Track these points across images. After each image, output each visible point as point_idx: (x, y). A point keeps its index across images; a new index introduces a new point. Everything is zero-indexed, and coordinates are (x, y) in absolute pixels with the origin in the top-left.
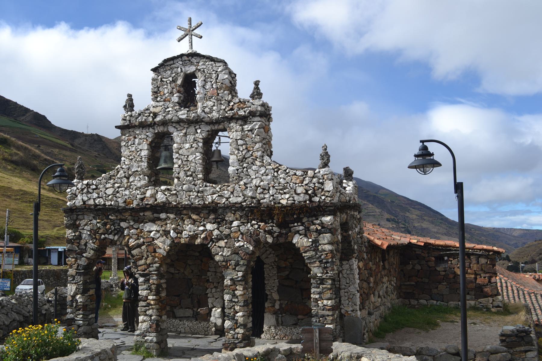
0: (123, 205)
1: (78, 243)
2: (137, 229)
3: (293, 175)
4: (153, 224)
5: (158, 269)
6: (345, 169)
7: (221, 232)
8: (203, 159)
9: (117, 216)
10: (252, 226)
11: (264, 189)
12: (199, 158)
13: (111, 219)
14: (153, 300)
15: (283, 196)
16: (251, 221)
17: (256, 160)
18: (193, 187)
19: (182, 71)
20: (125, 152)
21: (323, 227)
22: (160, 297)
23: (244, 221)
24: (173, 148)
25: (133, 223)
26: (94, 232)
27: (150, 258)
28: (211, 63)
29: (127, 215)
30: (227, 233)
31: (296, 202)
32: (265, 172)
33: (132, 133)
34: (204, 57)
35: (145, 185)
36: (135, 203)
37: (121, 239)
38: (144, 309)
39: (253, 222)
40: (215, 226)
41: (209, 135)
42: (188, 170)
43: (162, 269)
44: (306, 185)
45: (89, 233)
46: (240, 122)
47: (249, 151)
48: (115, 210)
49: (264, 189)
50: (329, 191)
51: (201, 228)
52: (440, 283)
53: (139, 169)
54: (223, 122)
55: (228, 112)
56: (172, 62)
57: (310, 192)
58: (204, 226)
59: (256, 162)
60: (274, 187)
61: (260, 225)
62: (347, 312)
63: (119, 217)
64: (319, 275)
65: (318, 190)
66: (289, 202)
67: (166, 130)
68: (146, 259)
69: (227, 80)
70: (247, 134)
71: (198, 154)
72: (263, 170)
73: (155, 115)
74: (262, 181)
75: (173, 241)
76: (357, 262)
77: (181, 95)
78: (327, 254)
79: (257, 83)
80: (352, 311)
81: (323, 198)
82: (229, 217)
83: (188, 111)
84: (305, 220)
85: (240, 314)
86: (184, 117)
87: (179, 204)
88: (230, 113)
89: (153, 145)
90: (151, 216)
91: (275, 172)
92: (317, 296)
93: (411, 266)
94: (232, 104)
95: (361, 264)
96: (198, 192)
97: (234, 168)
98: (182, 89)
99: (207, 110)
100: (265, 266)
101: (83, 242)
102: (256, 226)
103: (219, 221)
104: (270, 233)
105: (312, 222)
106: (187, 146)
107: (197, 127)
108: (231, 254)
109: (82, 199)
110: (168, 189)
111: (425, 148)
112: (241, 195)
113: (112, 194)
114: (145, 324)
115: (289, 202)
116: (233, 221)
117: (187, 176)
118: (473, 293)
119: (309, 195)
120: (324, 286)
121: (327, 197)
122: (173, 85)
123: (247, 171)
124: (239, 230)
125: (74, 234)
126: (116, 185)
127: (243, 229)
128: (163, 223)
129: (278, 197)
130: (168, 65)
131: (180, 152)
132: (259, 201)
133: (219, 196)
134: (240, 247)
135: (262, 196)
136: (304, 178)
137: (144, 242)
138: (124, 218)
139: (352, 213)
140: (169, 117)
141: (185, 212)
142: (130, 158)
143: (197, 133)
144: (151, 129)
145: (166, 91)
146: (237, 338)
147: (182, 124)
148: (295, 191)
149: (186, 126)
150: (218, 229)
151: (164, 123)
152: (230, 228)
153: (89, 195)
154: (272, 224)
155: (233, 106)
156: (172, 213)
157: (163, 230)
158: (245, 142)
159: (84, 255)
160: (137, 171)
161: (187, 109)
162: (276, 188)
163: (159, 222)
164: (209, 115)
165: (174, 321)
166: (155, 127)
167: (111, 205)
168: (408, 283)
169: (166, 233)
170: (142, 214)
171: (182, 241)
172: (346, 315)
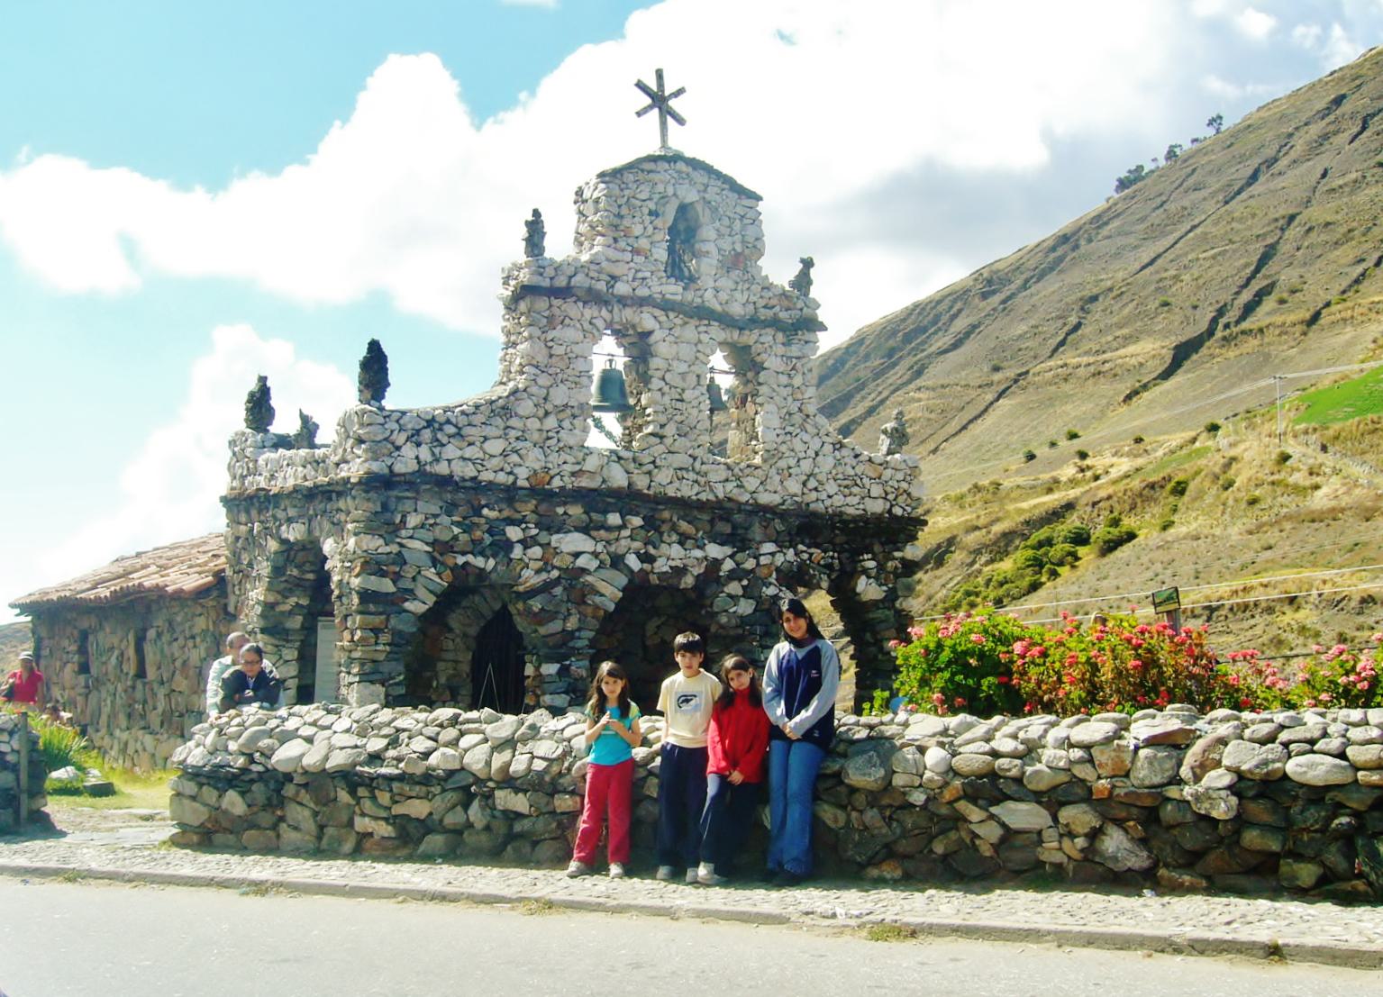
0: (526, 484)
1: (395, 573)
4: (584, 537)
7: (738, 564)
13: (487, 518)
15: (849, 500)
18: (691, 460)
19: (675, 194)
25: (536, 531)
26: (441, 549)
28: (731, 195)
34: (719, 175)
36: (557, 483)
39: (801, 547)
40: (728, 550)
46: (780, 336)
58: (702, 547)
61: (811, 555)
63: (506, 513)
68: (564, 620)
73: (614, 278)
79: (808, 264)
81: (909, 509)
82: (757, 532)
84: (877, 548)
87: (655, 495)
88: (765, 314)
90: (584, 517)
94: (766, 294)
101: (409, 572)
102: (805, 556)
103: (739, 541)
107: (702, 329)
108: (755, 610)
109: (417, 458)
122: (658, 222)
125: (388, 549)
126: (513, 434)
128: (614, 535)
130: (643, 171)
132: (808, 504)
135: (814, 495)
138: (518, 516)
141: (666, 515)
143: (700, 341)
144: (604, 312)
147: (672, 315)
149: (678, 321)
150: (732, 556)
152: (756, 557)
153: (437, 451)
156: (637, 514)
159: (407, 605)
166: (616, 310)
169: (617, 562)
170: (560, 510)
171: (654, 579)
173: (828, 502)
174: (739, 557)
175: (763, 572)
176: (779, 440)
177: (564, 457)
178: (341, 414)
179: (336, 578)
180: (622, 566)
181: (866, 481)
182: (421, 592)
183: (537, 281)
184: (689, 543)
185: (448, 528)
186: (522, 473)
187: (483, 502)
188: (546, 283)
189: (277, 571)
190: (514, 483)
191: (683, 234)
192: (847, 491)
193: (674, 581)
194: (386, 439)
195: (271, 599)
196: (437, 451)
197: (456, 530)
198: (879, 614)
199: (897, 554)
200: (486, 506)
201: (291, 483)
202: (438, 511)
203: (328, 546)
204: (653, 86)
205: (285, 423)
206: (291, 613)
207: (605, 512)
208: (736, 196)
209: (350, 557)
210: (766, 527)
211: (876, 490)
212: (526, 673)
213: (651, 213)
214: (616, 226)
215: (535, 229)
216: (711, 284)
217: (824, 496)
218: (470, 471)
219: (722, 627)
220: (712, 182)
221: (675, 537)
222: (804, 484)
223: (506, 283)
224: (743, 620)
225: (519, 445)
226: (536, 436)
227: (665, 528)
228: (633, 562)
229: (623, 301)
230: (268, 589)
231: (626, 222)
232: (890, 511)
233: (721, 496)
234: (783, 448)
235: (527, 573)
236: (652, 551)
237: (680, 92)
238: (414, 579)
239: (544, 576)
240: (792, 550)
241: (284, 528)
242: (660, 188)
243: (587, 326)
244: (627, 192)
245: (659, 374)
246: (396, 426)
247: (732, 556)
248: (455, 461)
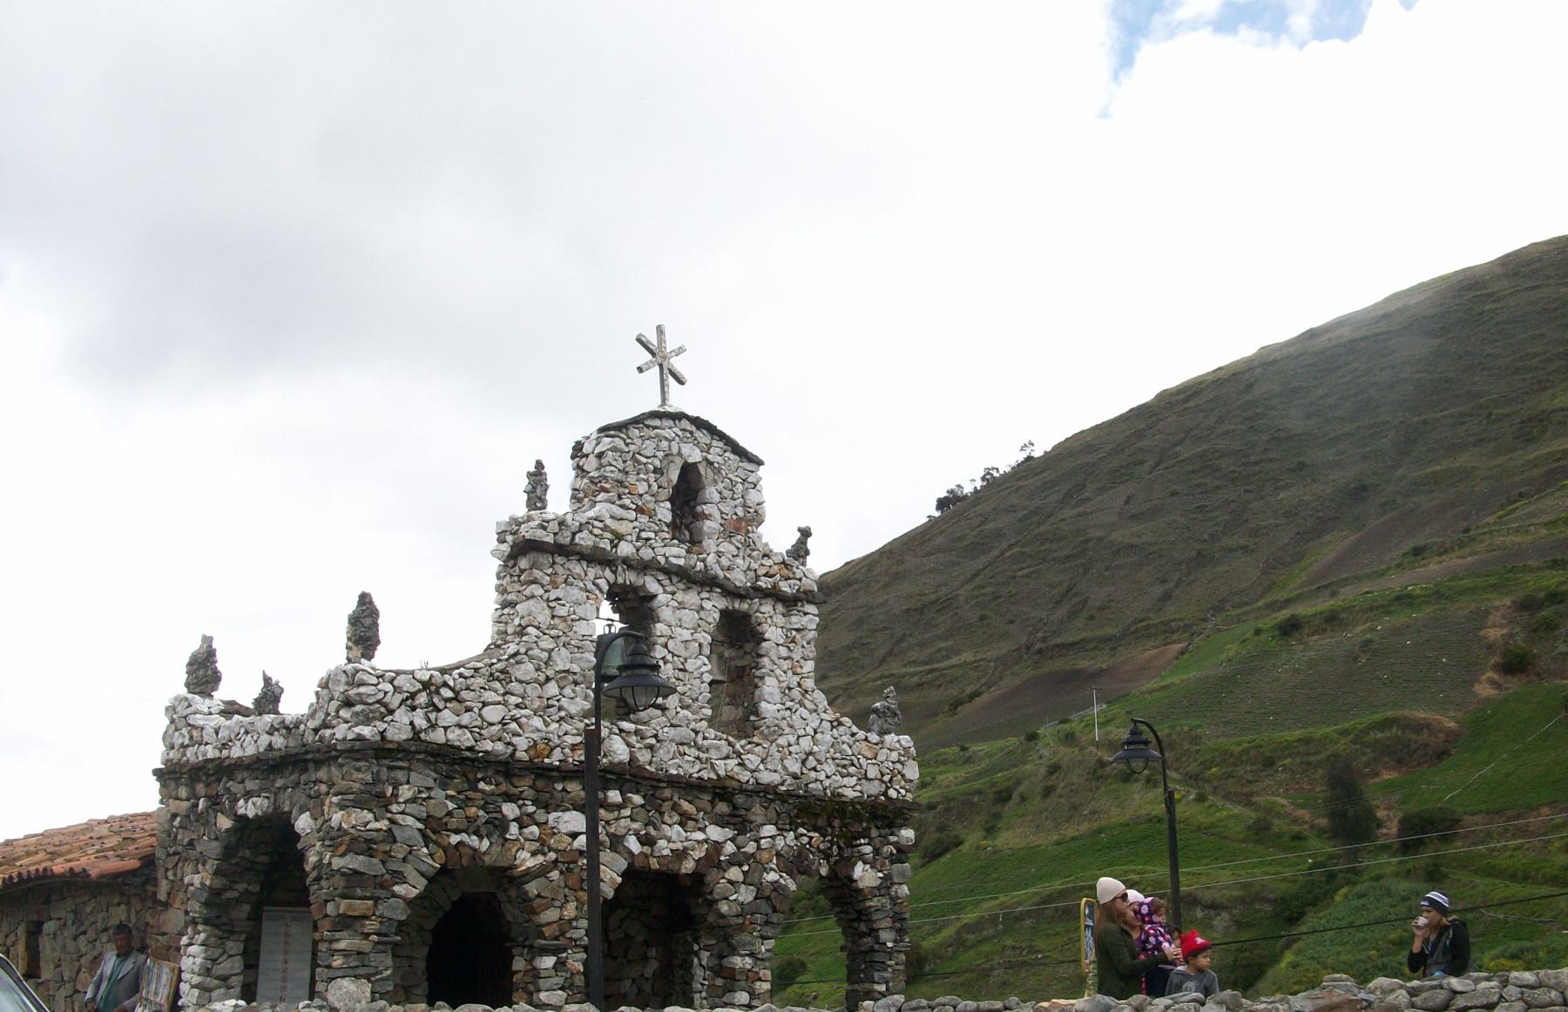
2: (538, 825)
13: (483, 792)
15: (846, 781)
19: (679, 454)
21: (899, 850)
26: (433, 827)
27: (572, 906)
28: (732, 457)
33: (560, 570)
34: (722, 436)
39: (802, 830)
40: (729, 832)
45: (421, 826)
46: (780, 607)
51: (700, 836)
56: (657, 422)
58: (702, 830)
63: (503, 788)
67: (640, 582)
73: (619, 537)
79: (805, 533)
82: (758, 813)
84: (874, 833)
86: (681, 562)
88: (764, 583)
99: (724, 561)
101: (399, 851)
102: (805, 840)
103: (740, 823)
104: (826, 855)
109: (412, 723)
112: (779, 767)
122: (663, 481)
125: (377, 825)
126: (513, 700)
127: (780, 842)
130: (648, 427)
135: (813, 774)
137: (556, 861)
140: (647, 554)
141: (667, 793)
142: (553, 632)
143: (702, 608)
144: (608, 573)
147: (675, 579)
149: (681, 586)
150: (733, 840)
152: (757, 841)
153: (432, 716)
156: (637, 792)
159: (396, 888)
160: (567, 671)
170: (559, 787)
171: (654, 864)
173: (827, 783)
174: (740, 839)
175: (765, 856)
176: (779, 715)
177: (566, 727)
178: (324, 674)
179: (312, 859)
180: (621, 849)
181: (862, 760)
182: (409, 871)
183: (541, 535)
185: (443, 801)
186: (522, 743)
187: (479, 776)
188: (550, 539)
189: (228, 852)
190: (512, 755)
191: (687, 494)
194: (378, 702)
195: (218, 883)
196: (432, 716)
197: (451, 806)
198: (874, 903)
199: (893, 839)
200: (483, 779)
201: (251, 750)
202: (430, 783)
203: (303, 823)
204: (652, 338)
205: (239, 686)
206: (238, 901)
207: (606, 789)
209: (333, 834)
212: (514, 968)
213: (656, 470)
215: (537, 480)
216: (714, 549)
217: (822, 777)
218: (466, 739)
219: (722, 916)
220: (715, 443)
221: (676, 818)
222: (804, 762)
223: (501, 541)
224: (745, 910)
225: (517, 713)
226: (537, 704)
227: (667, 806)
228: (633, 844)
229: (626, 561)
230: (217, 873)
231: (632, 479)
233: (722, 773)
234: (784, 724)
235: (524, 855)
236: (653, 832)
237: (680, 351)
238: (404, 860)
239: (540, 859)
241: (242, 802)
242: (665, 444)
243: (590, 586)
244: (632, 447)
245: (662, 640)
246: (389, 687)
247: (733, 840)
248: (451, 729)
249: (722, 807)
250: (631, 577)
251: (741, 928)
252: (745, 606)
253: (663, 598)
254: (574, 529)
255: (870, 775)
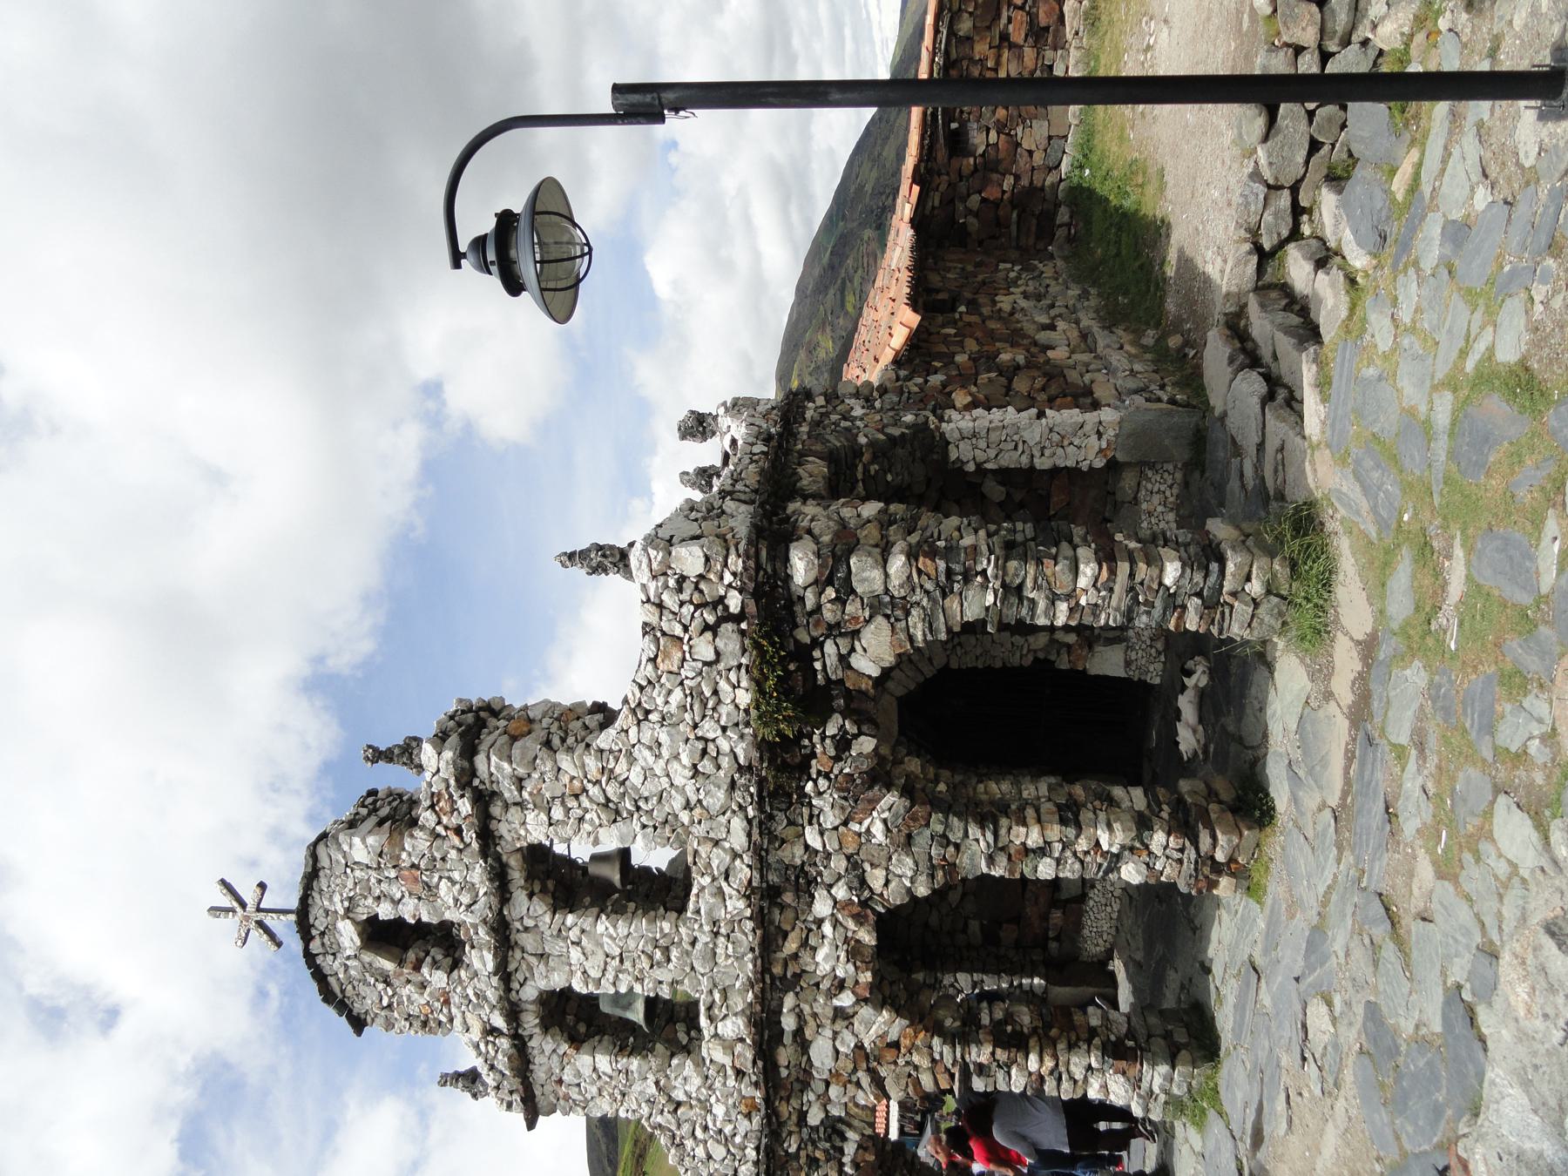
0: (756, 1119)
2: (828, 1084)
3: (656, 668)
5: (950, 1038)
6: (683, 437)
7: (840, 877)
8: (619, 910)
9: (790, 1133)
10: (820, 794)
11: (704, 752)
12: (611, 930)
13: (799, 1148)
14: (1041, 1060)
16: (806, 795)
17: (611, 771)
18: (699, 946)
20: (604, 1107)
22: (1034, 1030)
23: (806, 817)
24: (585, 991)
27: (916, 1058)
29: (784, 1109)
30: (844, 863)
31: (744, 661)
32: (650, 748)
33: (548, 1088)
35: (697, 1065)
36: (748, 1091)
37: (856, 1123)
38: (1065, 1085)
39: (809, 787)
40: (820, 895)
41: (544, 891)
42: (651, 957)
43: (948, 1022)
44: (686, 629)
46: (496, 810)
47: (585, 790)
48: (773, 1130)
49: (704, 752)
50: (707, 559)
51: (827, 928)
52: (1018, 145)
53: (651, 1078)
54: (498, 857)
55: (467, 840)
56: (331, 980)
57: (711, 619)
58: (819, 922)
59: (617, 771)
60: (695, 726)
61: (819, 773)
62: (1101, 451)
63: (794, 1128)
64: (990, 599)
65: (701, 592)
66: (744, 684)
68: (916, 1068)
69: (371, 840)
70: (531, 794)
71: (600, 928)
72: (644, 756)
73: (490, 1031)
74: (676, 757)
75: (866, 1000)
76: (954, 415)
77: (429, 959)
78: (920, 572)
80: (1100, 435)
81: (728, 578)
83: (473, 947)
84: (803, 637)
85: (1104, 838)
86: (489, 957)
88: (470, 835)
89: (582, 1028)
91: (646, 719)
92: (1063, 607)
93: (972, 220)
95: (961, 398)
96: (716, 934)
97: (639, 837)
98: (411, 956)
99: (465, 899)
100: (954, 665)
103: (804, 882)
104: (843, 744)
105: (810, 614)
106: (575, 954)
108: (910, 854)
110: (709, 1008)
111: (479, 243)
112: (723, 819)
113: (726, 1145)
114: (1112, 1086)
115: (744, 684)
116: (807, 847)
117: (669, 960)
118: (1049, 54)
119: (720, 621)
120: (1029, 583)
121: (726, 565)
123: (646, 799)
124: (836, 828)
126: (699, 1133)
127: (830, 819)
128: (811, 1023)
129: (728, 714)
130: (343, 991)
131: (594, 973)
132: (740, 769)
133: (726, 879)
134: (888, 830)
135: (725, 762)
136: (664, 634)
138: (794, 1118)
139: (804, 429)
141: (777, 970)
145: (419, 1002)
146: (1182, 850)
147: (511, 968)
148: (705, 664)
151: (513, 1012)
152: (828, 856)
154: (816, 738)
155: (446, 828)
157: (833, 1021)
158: (557, 802)
160: (657, 1083)
161: (467, 948)
162: (697, 719)
163: (808, 1033)
164: (481, 893)
165: (1091, 903)
167: (757, 1149)
168: (1014, 228)
169: (840, 1014)
170: (784, 1073)
171: (866, 977)
172: (1110, 454)
177: (717, 1085)
184: (812, 942)
192: (710, 704)
193: (868, 953)
208: (321, 873)
210: (783, 841)
211: (704, 649)
214: (425, 1024)
228: (846, 1000)
232: (737, 619)
234: (659, 816)
236: (825, 985)
240: (814, 802)
249: (788, 898)
250: (530, 1022)
251: (951, 868)
252: (514, 862)
253: (543, 984)
254: (498, 1077)
255: (711, 656)
